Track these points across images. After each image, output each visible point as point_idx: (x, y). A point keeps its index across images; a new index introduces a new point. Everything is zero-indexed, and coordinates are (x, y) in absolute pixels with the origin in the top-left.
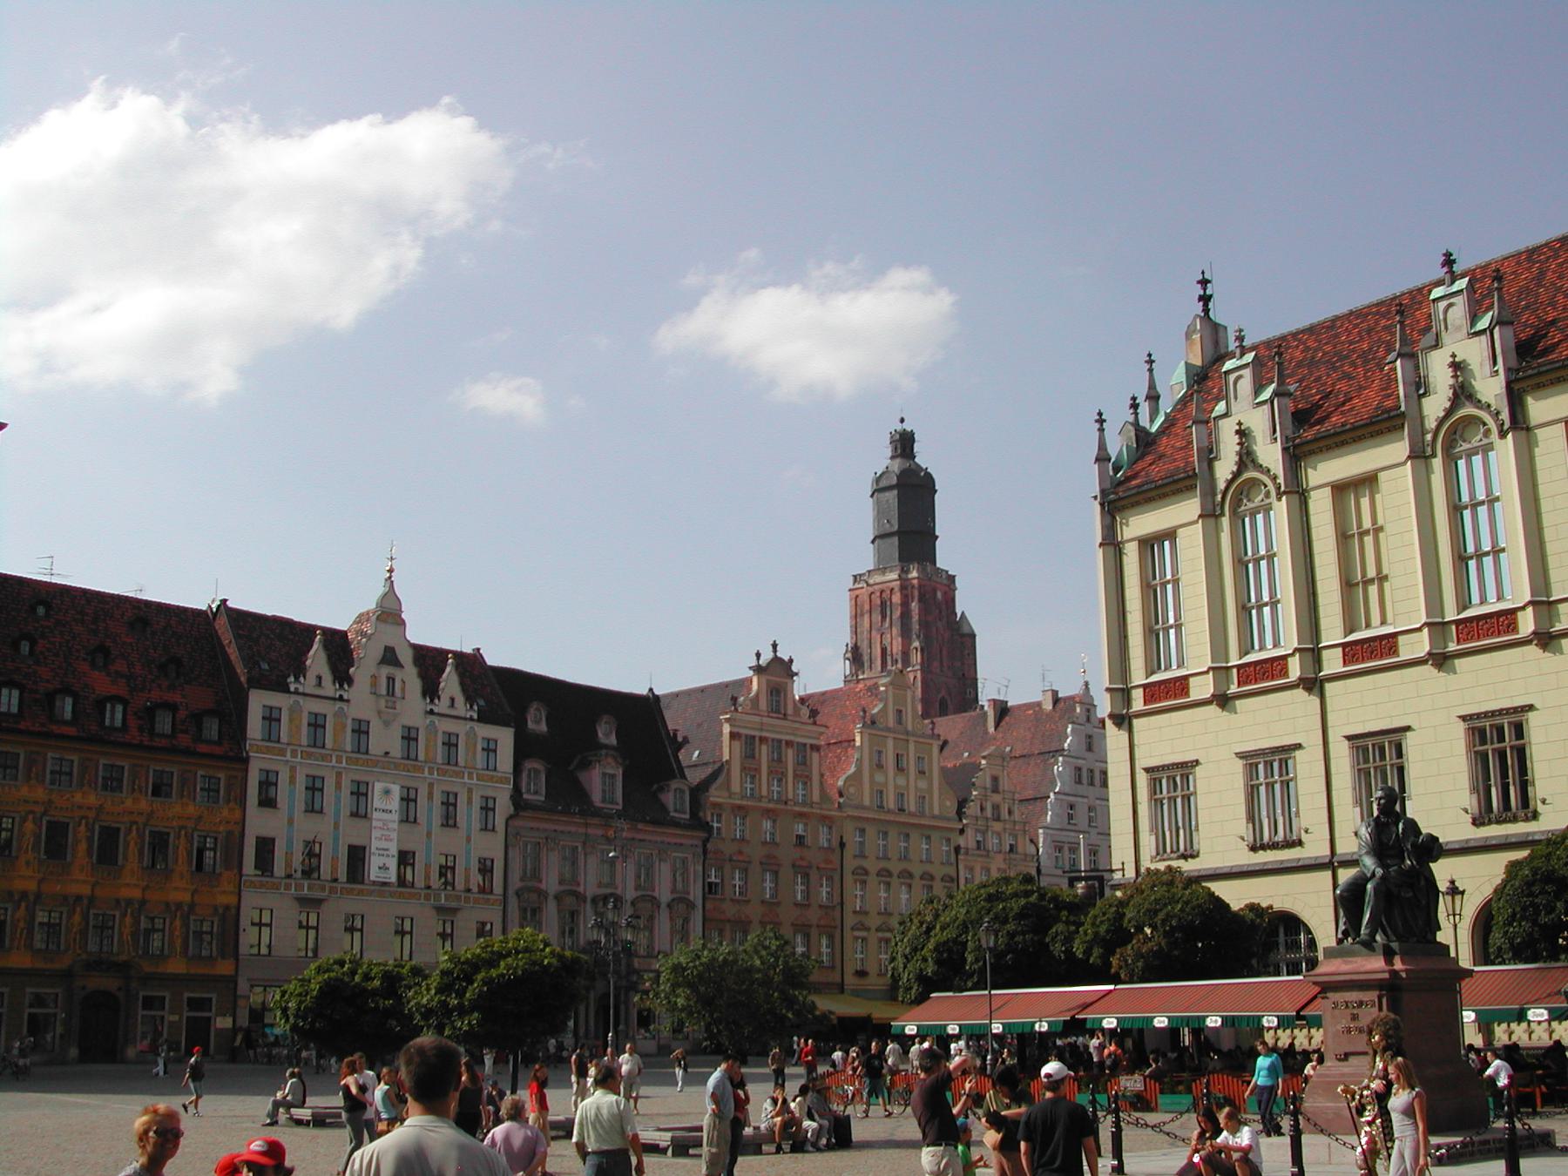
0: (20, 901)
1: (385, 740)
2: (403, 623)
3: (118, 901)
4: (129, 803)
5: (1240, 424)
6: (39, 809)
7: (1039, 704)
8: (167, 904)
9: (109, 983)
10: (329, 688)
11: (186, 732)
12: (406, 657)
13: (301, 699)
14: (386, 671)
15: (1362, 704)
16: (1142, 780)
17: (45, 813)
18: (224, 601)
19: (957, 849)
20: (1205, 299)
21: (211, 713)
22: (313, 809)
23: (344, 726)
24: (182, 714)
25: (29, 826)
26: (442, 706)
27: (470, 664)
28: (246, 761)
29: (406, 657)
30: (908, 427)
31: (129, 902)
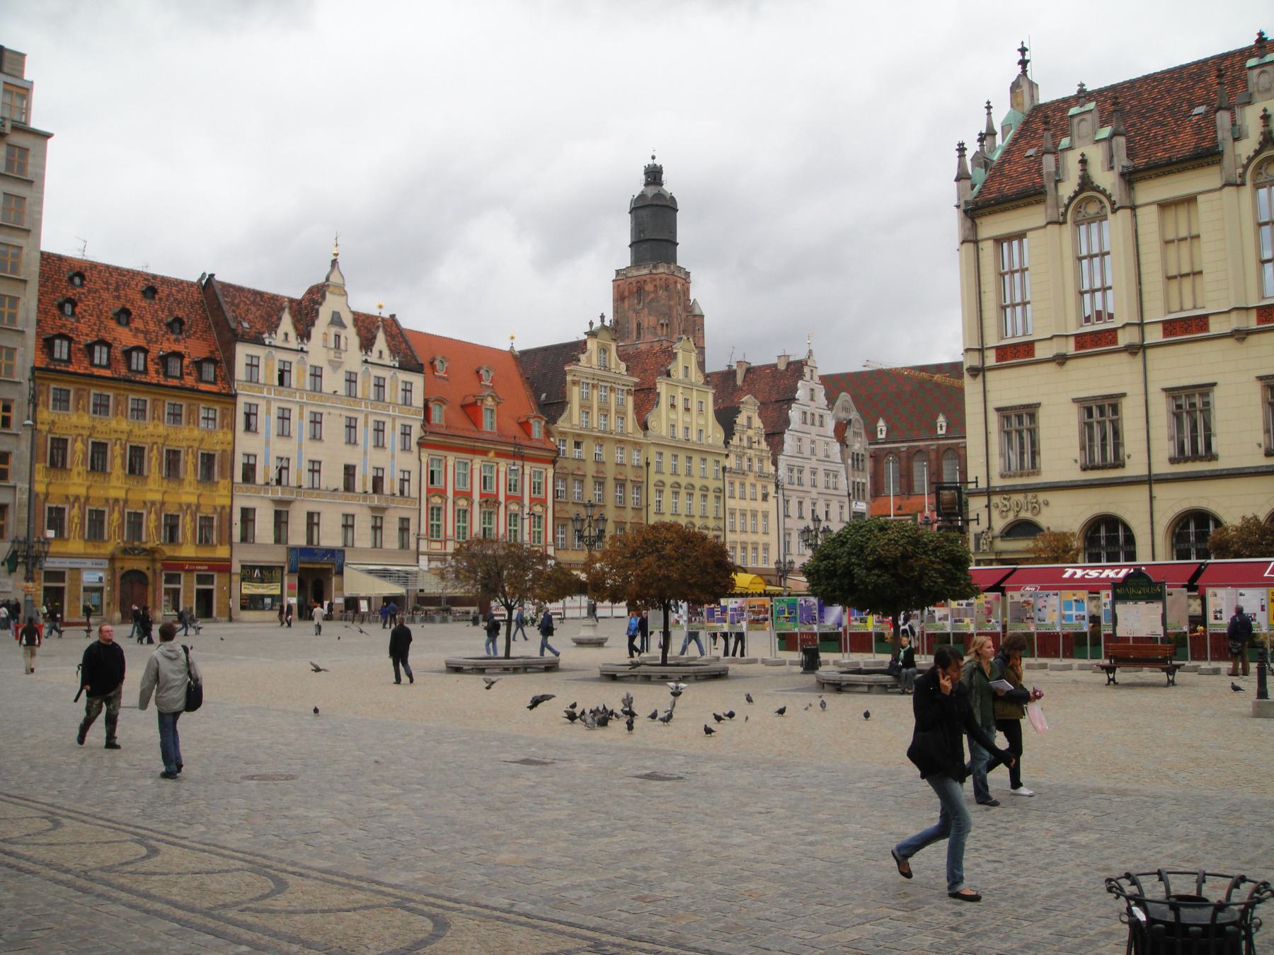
1: (333, 382)
2: (346, 294)
3: (145, 503)
4: (151, 428)
5: (1083, 155)
6: (85, 433)
7: (775, 366)
8: (180, 505)
9: (140, 565)
10: (294, 343)
11: (190, 374)
12: (348, 319)
13: (274, 351)
14: (333, 330)
15: (1181, 365)
16: (994, 418)
17: (90, 436)
18: (212, 276)
19: (724, 469)
20: (1024, 63)
21: (209, 360)
22: (284, 434)
23: (305, 371)
24: (186, 362)
25: (79, 445)
26: (373, 357)
27: (391, 325)
28: (235, 396)
29: (348, 319)
30: (658, 162)
31: (153, 503)
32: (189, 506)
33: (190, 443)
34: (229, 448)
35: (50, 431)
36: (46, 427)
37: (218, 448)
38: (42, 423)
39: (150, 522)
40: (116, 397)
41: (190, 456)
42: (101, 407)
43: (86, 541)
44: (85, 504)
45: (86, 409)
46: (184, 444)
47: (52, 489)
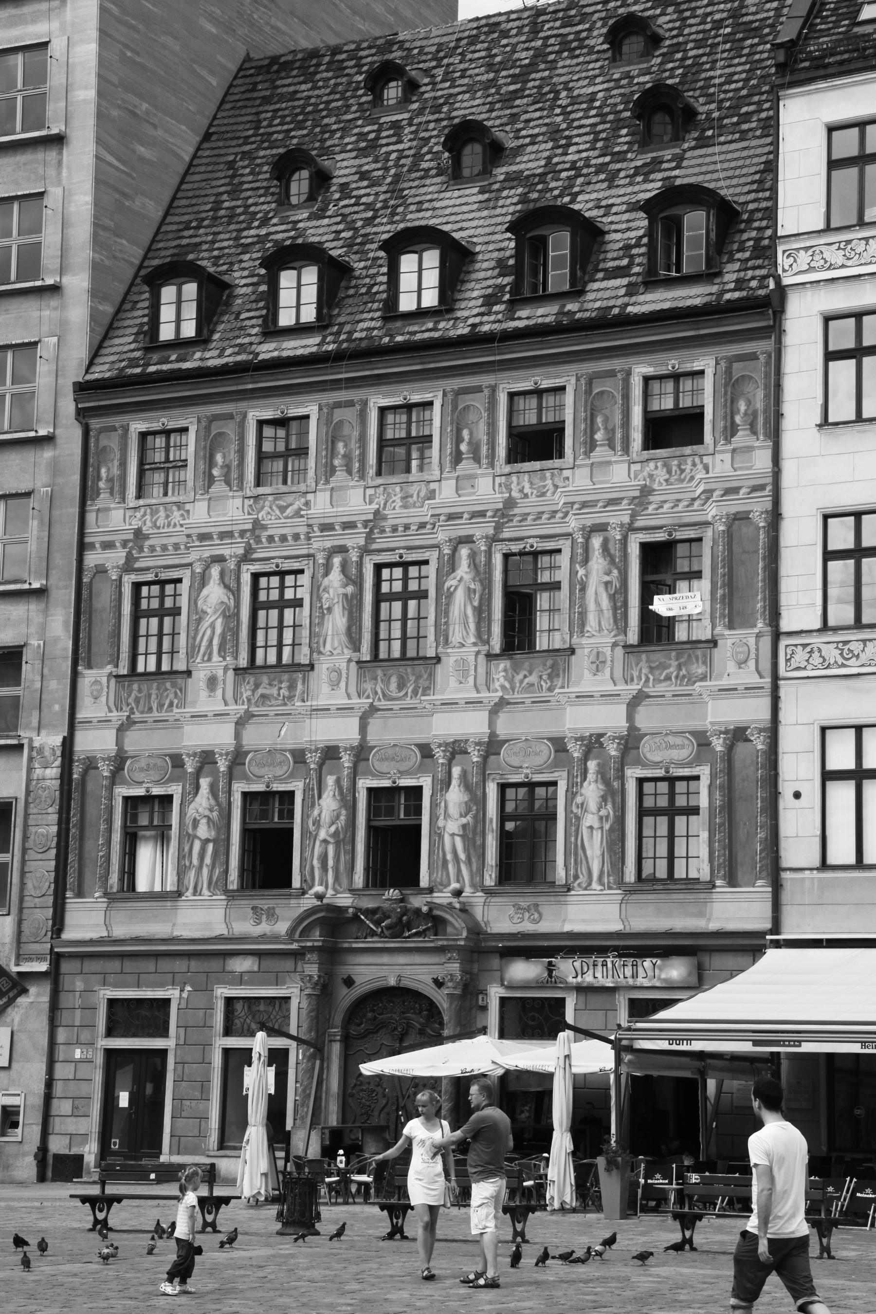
0: (198, 774)
3: (426, 751)
4: (447, 491)
6: (232, 550)
8: (559, 744)
17: (246, 558)
25: (214, 594)
31: (456, 749)
32: (593, 744)
33: (591, 519)
34: (759, 506)
35: (128, 567)
36: (118, 556)
37: (712, 511)
38: (108, 546)
39: (447, 820)
40: (326, 419)
41: (598, 563)
42: (282, 455)
43: (231, 896)
44: (231, 777)
45: (233, 478)
46: (573, 524)
47: (134, 741)
